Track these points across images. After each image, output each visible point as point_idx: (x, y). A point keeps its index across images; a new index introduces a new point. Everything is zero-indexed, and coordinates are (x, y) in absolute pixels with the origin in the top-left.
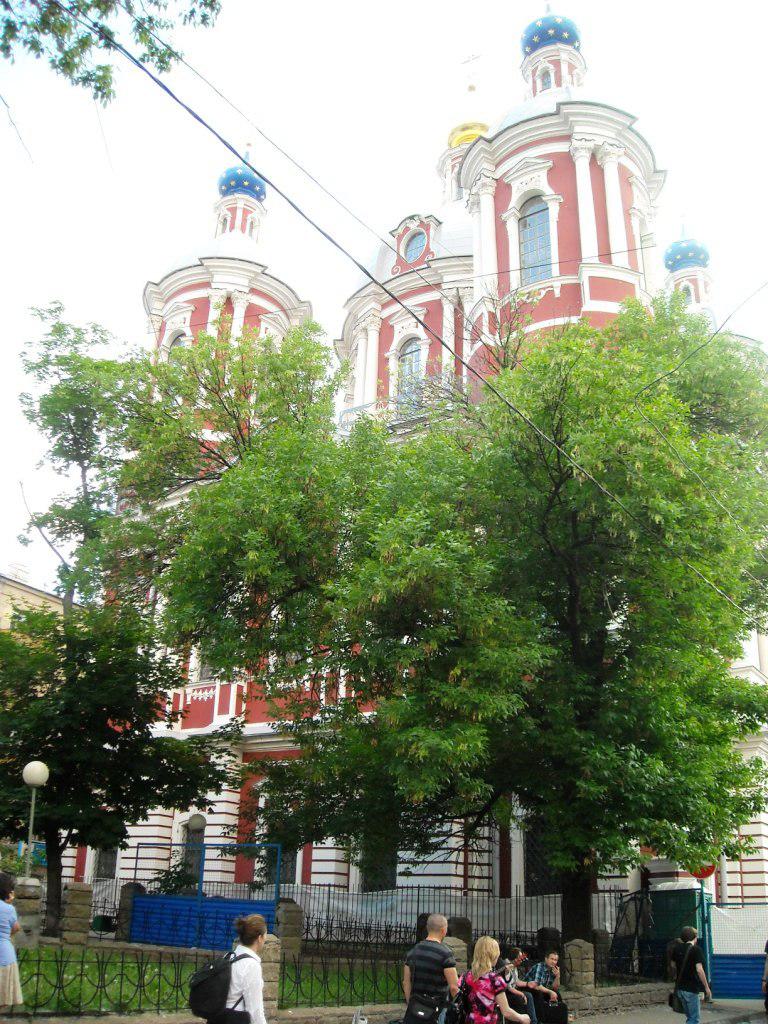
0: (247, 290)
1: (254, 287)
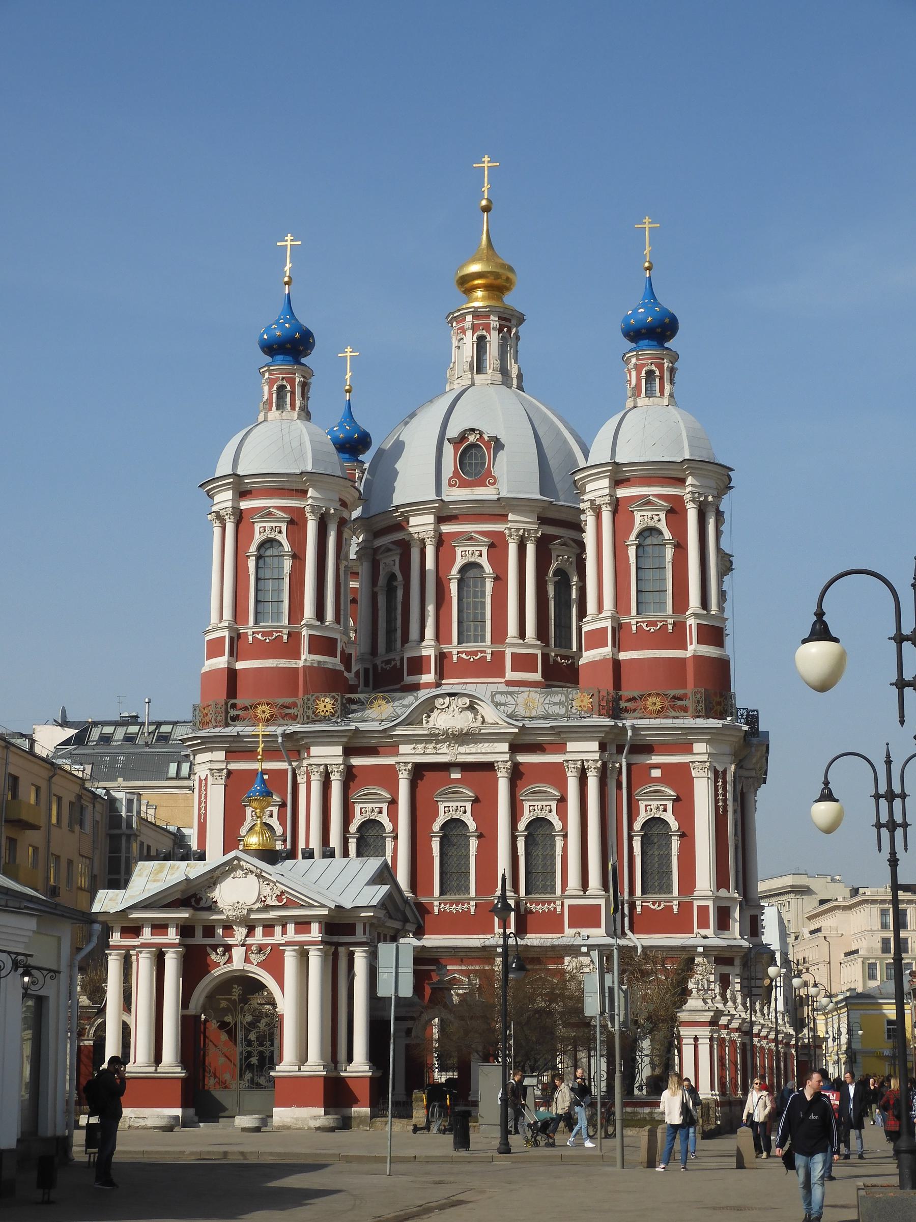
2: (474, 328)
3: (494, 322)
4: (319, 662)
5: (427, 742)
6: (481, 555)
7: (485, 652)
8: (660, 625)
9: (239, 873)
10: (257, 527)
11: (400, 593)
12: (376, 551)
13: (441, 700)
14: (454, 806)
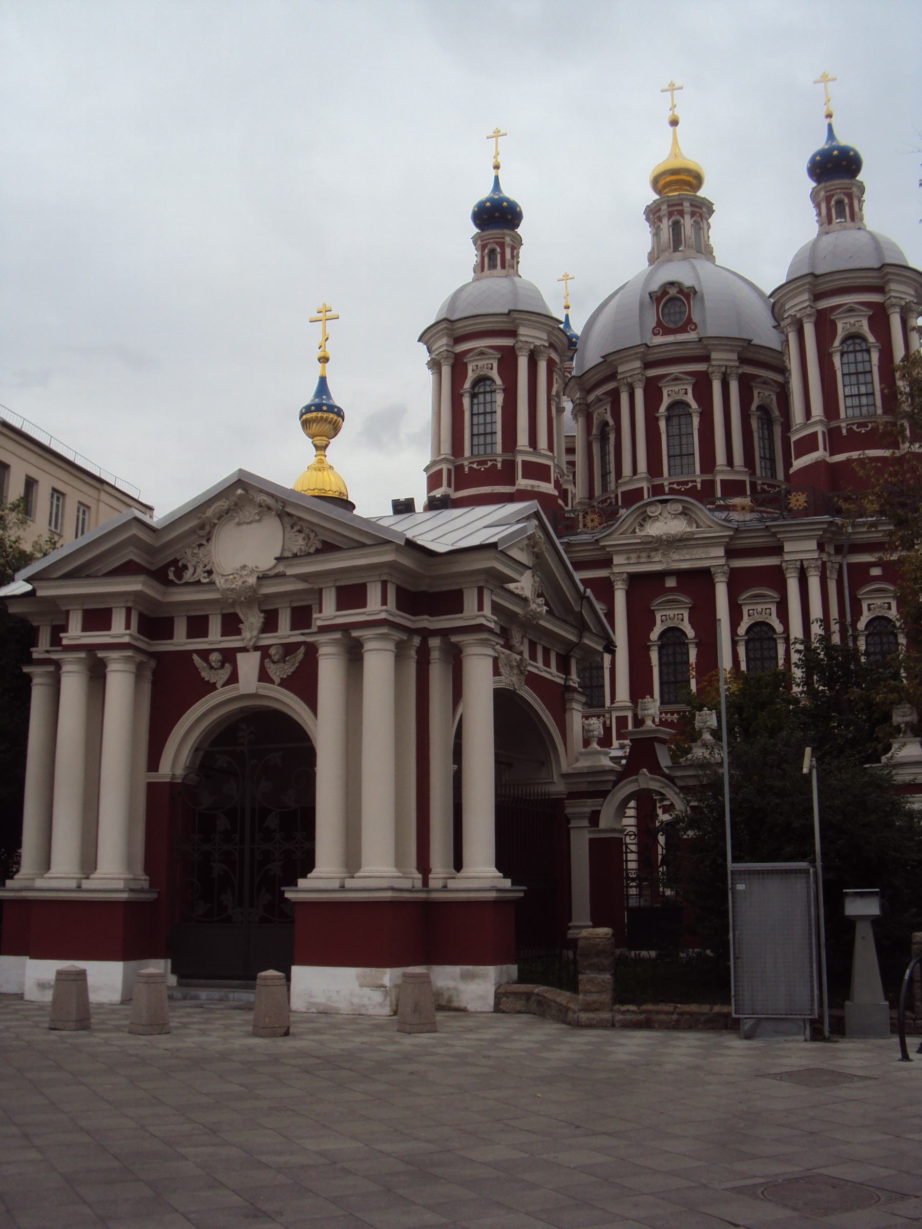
2: (670, 215)
3: (687, 207)
4: (533, 486)
5: (641, 551)
6: (686, 393)
7: (695, 481)
8: (870, 426)
9: (250, 513)
10: (470, 368)
11: (612, 437)
12: (588, 405)
13: (653, 509)
14: (673, 615)
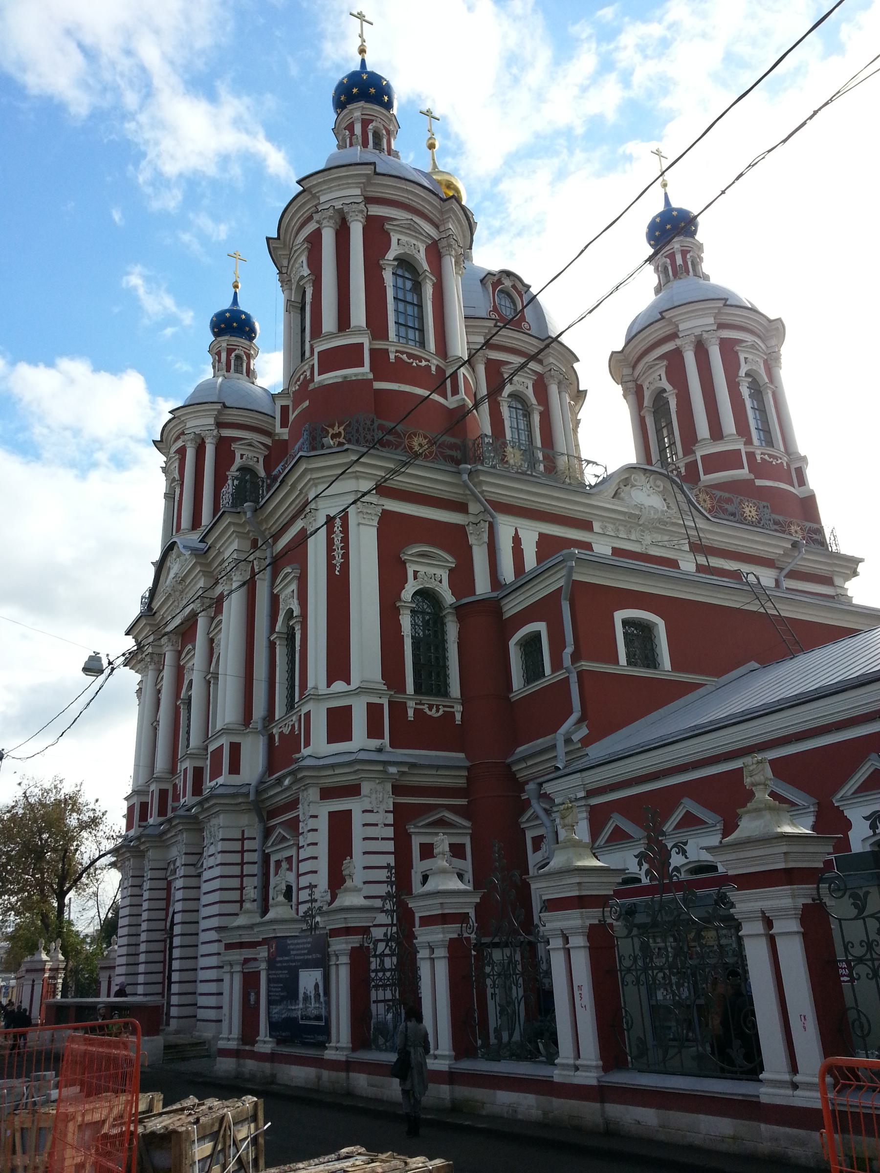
0: (715, 328)
1: (719, 321)
8: (780, 461)
